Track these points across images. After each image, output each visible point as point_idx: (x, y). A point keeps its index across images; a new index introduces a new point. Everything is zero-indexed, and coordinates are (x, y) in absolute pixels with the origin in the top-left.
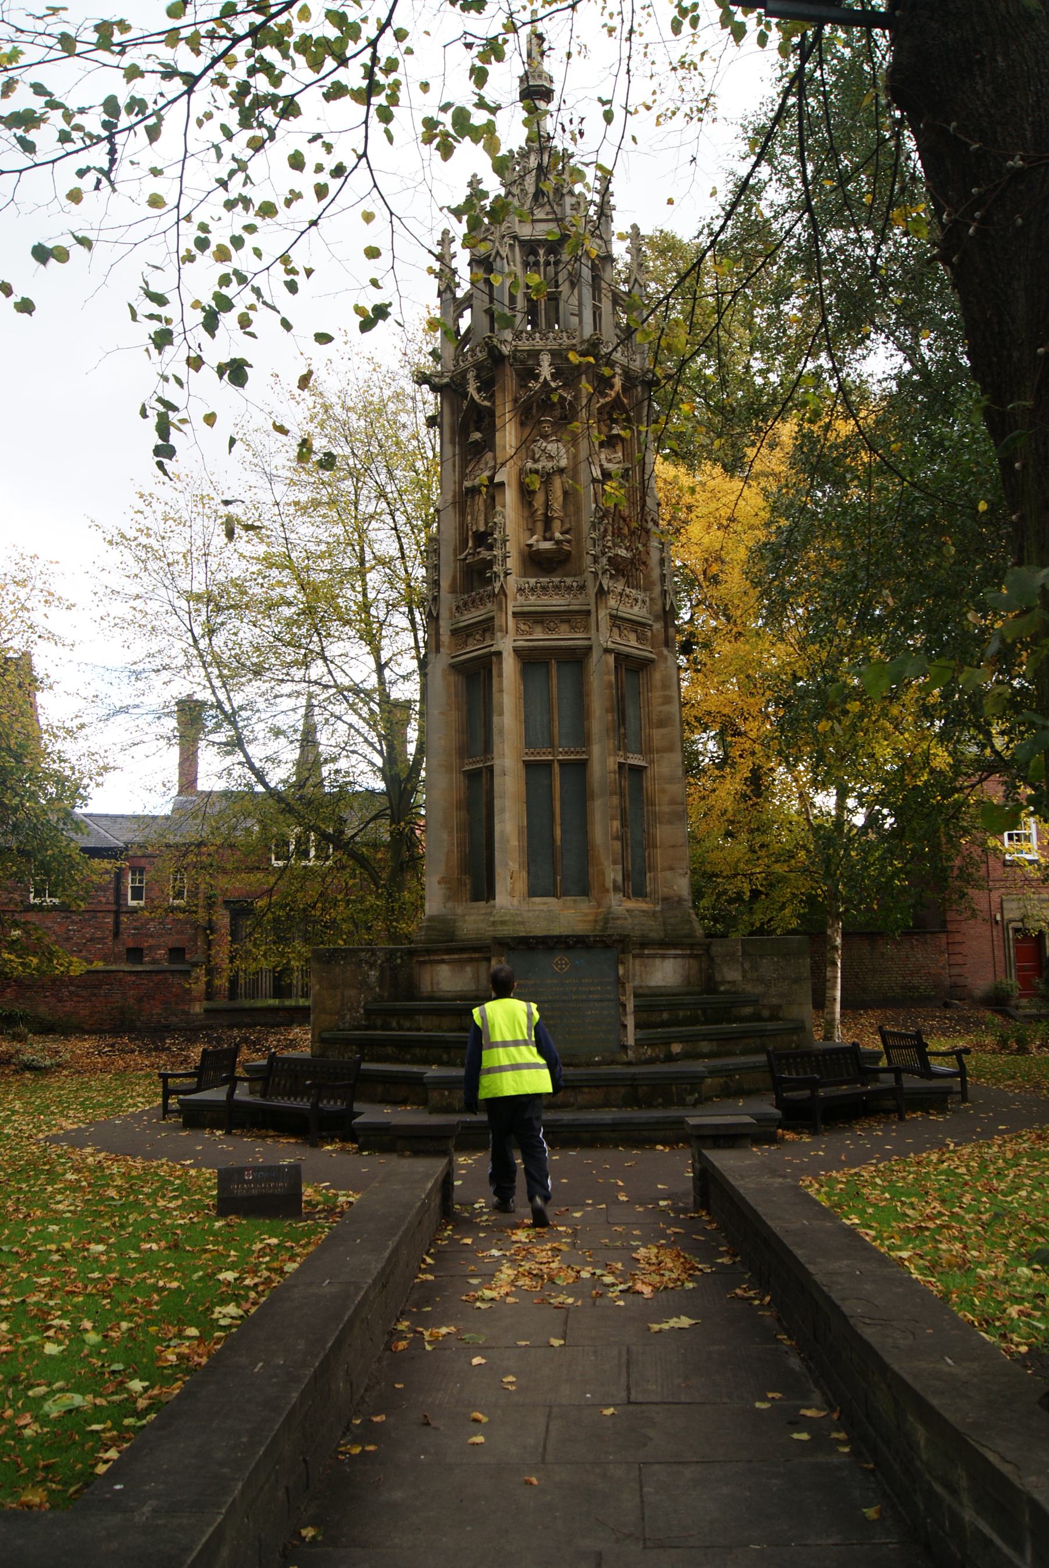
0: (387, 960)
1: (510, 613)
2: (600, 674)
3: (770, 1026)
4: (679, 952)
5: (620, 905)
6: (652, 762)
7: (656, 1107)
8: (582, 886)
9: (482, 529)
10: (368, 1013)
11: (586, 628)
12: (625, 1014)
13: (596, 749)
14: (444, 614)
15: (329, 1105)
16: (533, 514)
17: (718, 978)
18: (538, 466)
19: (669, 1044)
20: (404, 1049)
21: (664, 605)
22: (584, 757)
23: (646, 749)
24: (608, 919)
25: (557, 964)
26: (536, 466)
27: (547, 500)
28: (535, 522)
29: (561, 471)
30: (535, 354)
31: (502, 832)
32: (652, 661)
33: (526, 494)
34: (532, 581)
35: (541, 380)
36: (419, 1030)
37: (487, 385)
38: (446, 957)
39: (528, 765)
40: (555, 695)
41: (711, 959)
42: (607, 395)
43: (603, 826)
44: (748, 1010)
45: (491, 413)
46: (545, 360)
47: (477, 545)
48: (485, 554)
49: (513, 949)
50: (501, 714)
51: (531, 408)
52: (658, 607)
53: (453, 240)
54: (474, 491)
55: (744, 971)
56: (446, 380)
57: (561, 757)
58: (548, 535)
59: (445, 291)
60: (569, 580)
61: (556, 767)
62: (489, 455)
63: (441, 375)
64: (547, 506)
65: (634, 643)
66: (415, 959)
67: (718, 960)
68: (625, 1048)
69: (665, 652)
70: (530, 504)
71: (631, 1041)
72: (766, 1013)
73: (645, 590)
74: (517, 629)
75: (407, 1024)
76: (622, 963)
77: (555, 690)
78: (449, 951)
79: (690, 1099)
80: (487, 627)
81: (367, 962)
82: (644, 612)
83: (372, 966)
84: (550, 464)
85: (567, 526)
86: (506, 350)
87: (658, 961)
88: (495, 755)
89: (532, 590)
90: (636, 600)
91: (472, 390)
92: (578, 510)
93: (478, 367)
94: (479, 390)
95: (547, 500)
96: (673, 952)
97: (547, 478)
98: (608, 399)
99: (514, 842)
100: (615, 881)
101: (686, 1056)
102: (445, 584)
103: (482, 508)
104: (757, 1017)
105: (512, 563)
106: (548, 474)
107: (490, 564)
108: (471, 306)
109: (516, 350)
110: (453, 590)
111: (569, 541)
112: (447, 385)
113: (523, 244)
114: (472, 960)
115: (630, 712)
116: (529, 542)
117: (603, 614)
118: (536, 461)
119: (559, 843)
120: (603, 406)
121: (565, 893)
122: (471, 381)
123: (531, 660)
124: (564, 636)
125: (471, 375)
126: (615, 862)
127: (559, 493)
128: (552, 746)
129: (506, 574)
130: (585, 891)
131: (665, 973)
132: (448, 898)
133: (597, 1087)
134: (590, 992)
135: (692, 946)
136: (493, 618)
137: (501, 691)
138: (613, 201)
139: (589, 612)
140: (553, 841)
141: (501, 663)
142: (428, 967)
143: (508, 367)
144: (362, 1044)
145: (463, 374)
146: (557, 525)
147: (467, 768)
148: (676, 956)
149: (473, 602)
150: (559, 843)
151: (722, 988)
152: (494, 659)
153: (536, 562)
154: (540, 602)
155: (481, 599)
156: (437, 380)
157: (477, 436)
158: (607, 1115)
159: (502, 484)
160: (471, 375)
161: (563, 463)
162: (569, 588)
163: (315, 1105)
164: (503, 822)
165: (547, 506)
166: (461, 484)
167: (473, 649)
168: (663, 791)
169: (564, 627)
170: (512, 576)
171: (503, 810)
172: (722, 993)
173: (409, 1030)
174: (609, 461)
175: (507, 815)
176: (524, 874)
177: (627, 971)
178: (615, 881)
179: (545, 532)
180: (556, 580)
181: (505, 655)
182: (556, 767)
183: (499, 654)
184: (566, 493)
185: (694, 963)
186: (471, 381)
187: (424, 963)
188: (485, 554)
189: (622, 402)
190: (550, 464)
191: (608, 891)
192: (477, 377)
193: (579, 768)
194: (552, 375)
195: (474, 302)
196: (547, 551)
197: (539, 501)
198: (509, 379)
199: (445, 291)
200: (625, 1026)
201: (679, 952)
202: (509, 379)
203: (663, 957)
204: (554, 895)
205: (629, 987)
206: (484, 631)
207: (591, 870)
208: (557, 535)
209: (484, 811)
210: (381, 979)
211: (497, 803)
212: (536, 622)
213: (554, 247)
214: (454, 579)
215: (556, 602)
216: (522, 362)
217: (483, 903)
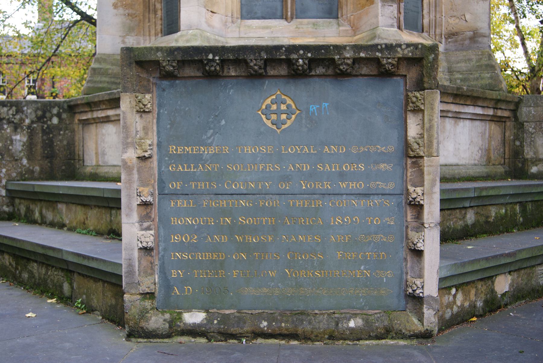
0: (40, 119)
12: (420, 226)
17: (529, 153)
19: (491, 278)
25: (267, 112)
41: (520, 126)
49: (169, 76)
66: (78, 117)
67: (530, 128)
68: (416, 300)
71: (430, 287)
76: (417, 111)
81: (9, 122)
83: (16, 127)
96: (471, 110)
132: (130, 30)
134: (342, 176)
135: (497, 103)
142: (93, 128)
148: (474, 118)
151: (534, 169)
177: (427, 131)
185: (495, 129)
187: (86, 123)
200: (418, 254)
201: (479, 111)
203: (457, 117)
204: (283, 17)
205: (431, 169)
210: (30, 146)
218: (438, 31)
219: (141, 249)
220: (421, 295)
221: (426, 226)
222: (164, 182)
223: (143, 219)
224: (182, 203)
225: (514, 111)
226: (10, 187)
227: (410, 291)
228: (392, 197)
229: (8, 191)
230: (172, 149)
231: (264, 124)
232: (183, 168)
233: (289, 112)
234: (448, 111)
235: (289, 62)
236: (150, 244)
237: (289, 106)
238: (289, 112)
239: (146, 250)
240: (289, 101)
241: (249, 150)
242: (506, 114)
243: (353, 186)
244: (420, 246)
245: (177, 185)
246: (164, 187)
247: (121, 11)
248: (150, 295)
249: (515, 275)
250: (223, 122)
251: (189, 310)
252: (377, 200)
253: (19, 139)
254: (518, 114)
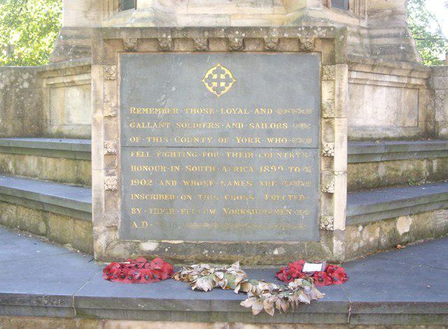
17: (439, 117)
19: (394, 219)
68: (329, 234)
87: (367, 90)
96: (387, 78)
134: (270, 133)
148: (391, 86)
185: (408, 94)
200: (330, 196)
201: (394, 79)
203: (375, 85)
218: (362, 8)
219: (107, 190)
220: (331, 229)
221: (336, 173)
222: (125, 137)
223: (109, 167)
224: (139, 154)
225: (427, 80)
227: (323, 226)
228: (310, 150)
230: (133, 110)
231: (207, 90)
232: (141, 125)
234: (367, 80)
235: (227, 40)
236: (114, 187)
237: (227, 76)
238: (227, 80)
240: (227, 72)
241: (194, 111)
242: (419, 82)
243: (279, 141)
244: (331, 190)
245: (136, 140)
246: (125, 142)
249: (416, 217)
250: (174, 89)
251: (145, 240)
252: (297, 153)
254: (430, 82)
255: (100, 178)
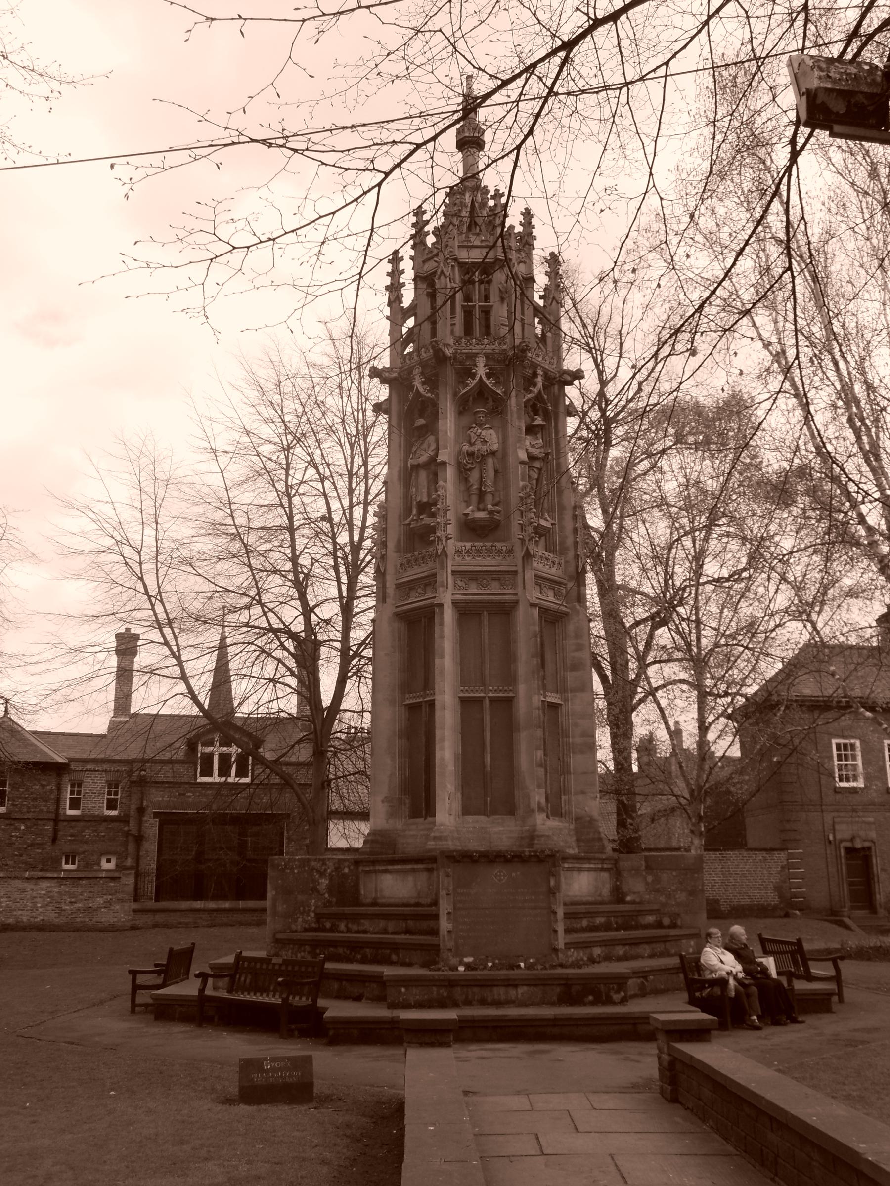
1: (449, 571)
2: (526, 622)
3: (673, 932)
4: (592, 866)
5: (544, 823)
6: (566, 700)
7: (585, 1004)
8: (507, 806)
9: (425, 499)
10: (319, 917)
11: (514, 585)
13: (522, 688)
14: (390, 570)
15: (299, 1001)
16: (468, 489)
17: (625, 889)
18: (475, 449)
20: (354, 950)
21: (577, 567)
22: (511, 695)
23: (562, 689)
24: (532, 836)
25: (496, 876)
26: (472, 449)
27: (481, 477)
28: (470, 495)
29: (493, 453)
30: (473, 357)
31: (442, 759)
32: (566, 614)
33: (463, 472)
34: (468, 545)
35: (478, 378)
36: (365, 932)
37: (432, 382)
38: (390, 867)
39: (464, 701)
40: (487, 641)
42: (531, 392)
43: (528, 755)
44: (650, 919)
45: (434, 404)
46: (481, 362)
47: (420, 513)
48: (427, 520)
49: (458, 862)
50: (442, 657)
51: (468, 401)
52: (572, 569)
53: (402, 259)
54: (417, 467)
55: (647, 883)
56: (395, 375)
57: (491, 695)
58: (481, 506)
59: (394, 301)
60: (499, 545)
61: (487, 703)
62: (431, 438)
63: (390, 369)
64: (481, 482)
65: (551, 599)
67: (625, 874)
68: (556, 950)
69: (578, 607)
70: (466, 480)
72: (666, 921)
73: (561, 554)
74: (455, 585)
75: (355, 927)
76: (554, 875)
77: (486, 638)
78: (393, 862)
79: (616, 997)
80: (430, 582)
81: (318, 871)
82: (560, 573)
83: (322, 874)
84: (484, 448)
85: (497, 499)
86: (449, 352)
87: (575, 874)
88: (437, 690)
89: (468, 552)
90: (554, 563)
91: (417, 383)
92: (506, 487)
93: (423, 364)
94: (423, 383)
95: (481, 477)
96: (587, 866)
97: (480, 459)
98: (529, 396)
99: (451, 767)
100: (539, 803)
101: (608, 958)
102: (391, 545)
103: (425, 484)
104: (659, 925)
105: (451, 529)
106: (483, 456)
107: (433, 530)
108: (415, 315)
109: (456, 353)
110: (398, 551)
111: (499, 512)
112: (395, 379)
113: (461, 265)
114: (414, 870)
115: (548, 656)
116: (466, 512)
117: (529, 575)
118: (472, 445)
119: (489, 769)
120: (529, 400)
121: (494, 812)
122: (417, 377)
123: (467, 612)
124: (495, 592)
125: (417, 371)
126: (539, 787)
127: (491, 473)
128: (484, 685)
129: (448, 538)
130: (511, 811)
131: (581, 884)
133: (535, 985)
135: (603, 861)
136: (435, 575)
137: (442, 637)
138: (535, 232)
139: (516, 572)
140: (484, 766)
141: (442, 613)
142: (374, 875)
143: (449, 368)
144: (315, 945)
145: (410, 371)
146: (489, 498)
147: (408, 702)
148: (589, 870)
149: (416, 560)
150: (489, 769)
151: (628, 899)
152: (437, 610)
153: (472, 529)
154: (475, 563)
155: (423, 558)
156: (387, 374)
157: (421, 422)
158: (548, 1012)
159: (444, 463)
160: (417, 371)
161: (495, 447)
162: (500, 551)
163: (285, 1000)
164: (442, 749)
165: (481, 482)
166: (406, 462)
167: (416, 600)
168: (576, 725)
169: (495, 584)
170: (451, 540)
171: (443, 740)
172: (629, 903)
173: (358, 932)
174: (533, 446)
175: (447, 744)
176: (459, 795)
178: (539, 803)
179: (479, 503)
180: (489, 544)
181: (446, 606)
182: (487, 703)
183: (441, 606)
184: (496, 472)
186: (417, 377)
188: (427, 520)
189: (542, 397)
190: (484, 448)
191: (533, 811)
192: (422, 373)
193: (506, 704)
194: (486, 374)
195: (418, 311)
196: (481, 520)
197: (474, 476)
198: (450, 375)
199: (394, 301)
200: (556, 931)
201: (592, 866)
202: (450, 375)
203: (580, 870)
204: (485, 814)
206: (426, 585)
207: (516, 792)
208: (490, 506)
209: (423, 739)
211: (438, 733)
212: (471, 579)
213: (486, 269)
214: (399, 541)
215: (488, 563)
216: (461, 363)
217: (421, 820)
223: (448, 919)
225: (615, 864)
226: (318, 911)
229: (316, 914)
230: (460, 891)
233: (504, 876)
235: (505, 856)
238: (504, 876)
239: (449, 932)
242: (609, 866)
247: (386, 804)
248: (450, 950)
249: (604, 948)
251: (466, 957)
253: (324, 882)
255: (445, 925)
